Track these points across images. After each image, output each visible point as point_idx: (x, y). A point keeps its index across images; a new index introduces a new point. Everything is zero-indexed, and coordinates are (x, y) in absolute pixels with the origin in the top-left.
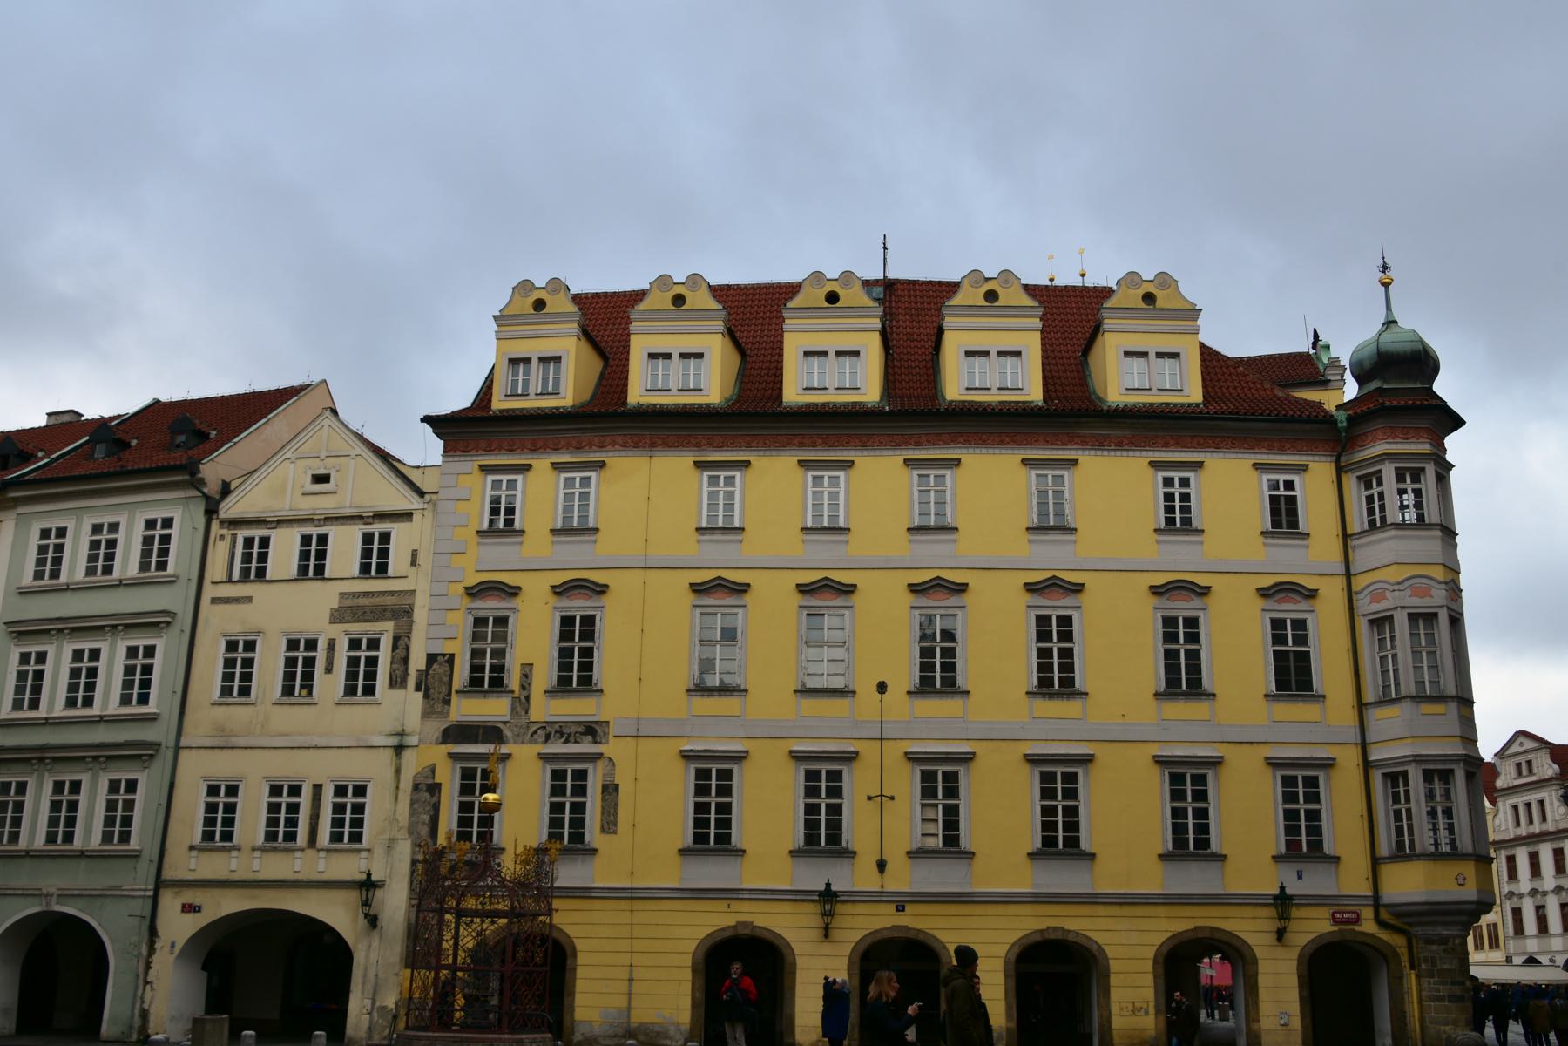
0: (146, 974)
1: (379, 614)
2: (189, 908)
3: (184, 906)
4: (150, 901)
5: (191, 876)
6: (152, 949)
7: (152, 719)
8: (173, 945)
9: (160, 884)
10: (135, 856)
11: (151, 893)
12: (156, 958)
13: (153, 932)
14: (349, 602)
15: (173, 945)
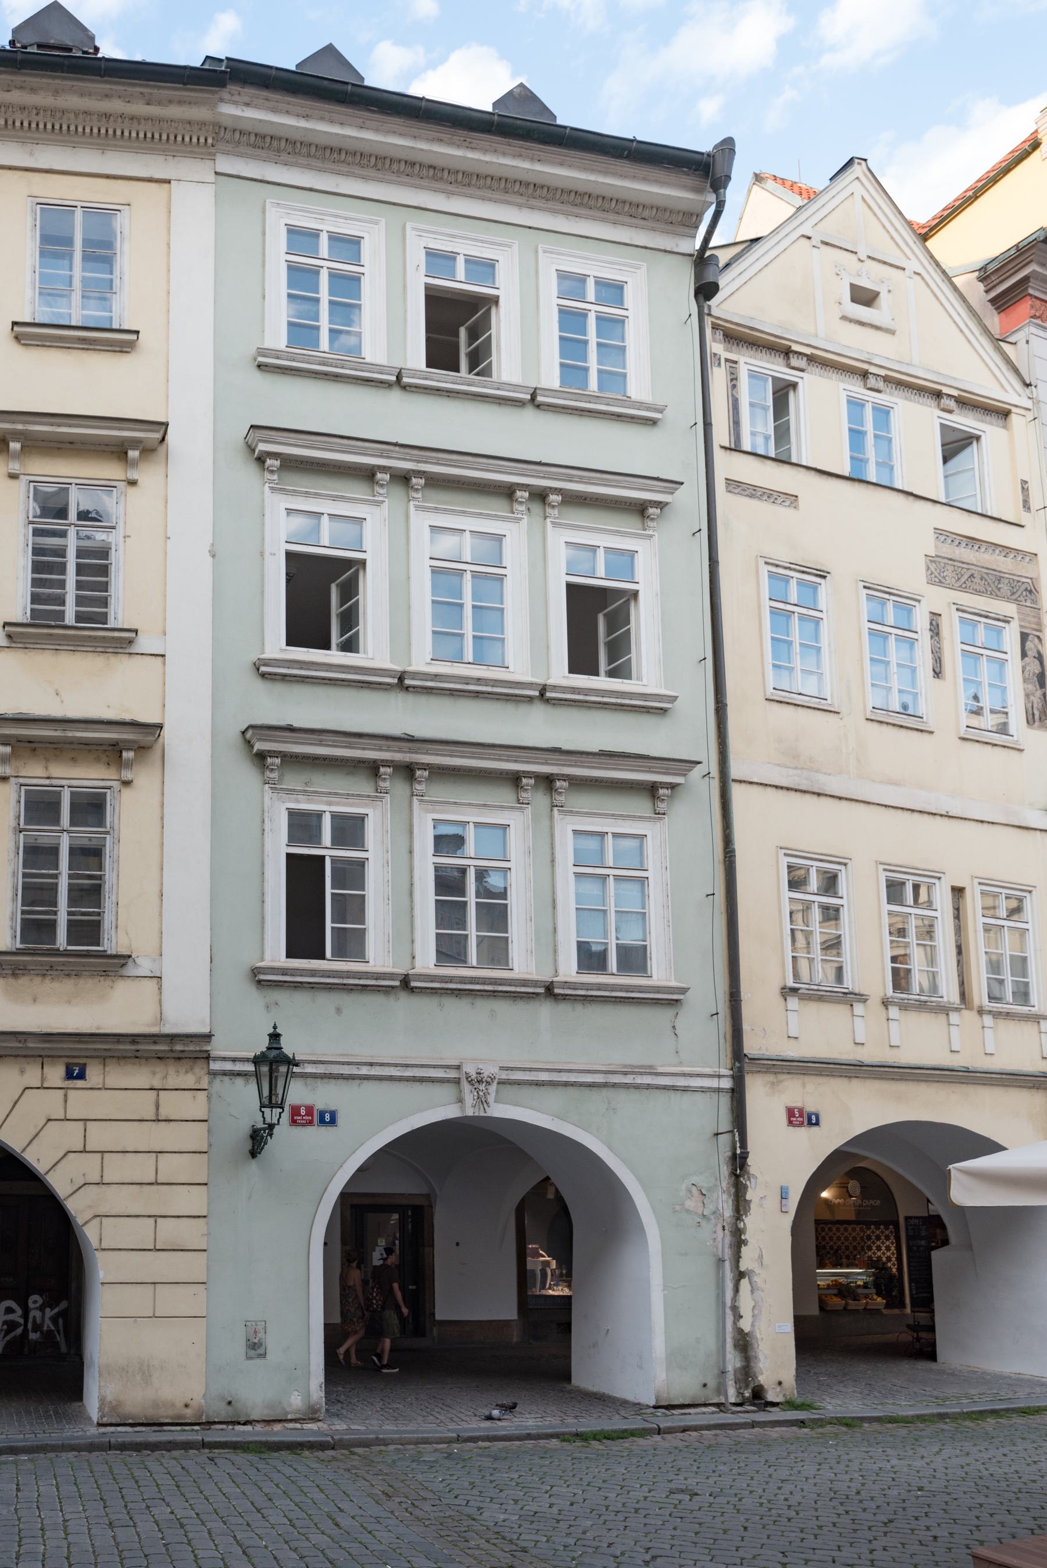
0: (737, 1257)
1: (991, 583)
2: (802, 1118)
3: (790, 1112)
4: (725, 1101)
5: (792, 1051)
6: (740, 1205)
7: (654, 708)
8: (784, 1196)
9: (740, 1061)
10: (669, 1001)
11: (727, 1084)
12: (751, 1223)
13: (739, 1163)
14: (948, 550)
15: (784, 1196)
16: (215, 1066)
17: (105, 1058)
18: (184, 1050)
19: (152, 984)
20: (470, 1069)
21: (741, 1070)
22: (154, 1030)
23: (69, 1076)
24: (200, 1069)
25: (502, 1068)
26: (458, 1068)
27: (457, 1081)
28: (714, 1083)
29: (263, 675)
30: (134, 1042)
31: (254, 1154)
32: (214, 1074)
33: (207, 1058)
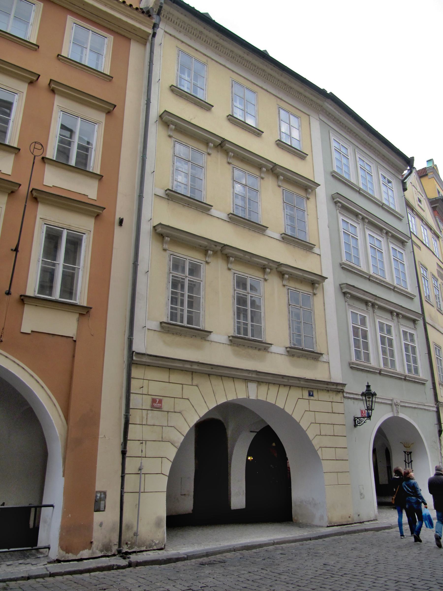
4: (435, 415)
10: (422, 383)
11: (435, 409)
16: (345, 395)
17: (318, 389)
18: (336, 388)
19: (326, 365)
20: (395, 401)
21: (438, 405)
22: (329, 380)
23: (310, 395)
24: (340, 395)
25: (401, 402)
26: (392, 400)
27: (391, 405)
28: (431, 409)
29: (343, 268)
30: (327, 384)
31: (355, 426)
32: (344, 397)
33: (343, 392)
